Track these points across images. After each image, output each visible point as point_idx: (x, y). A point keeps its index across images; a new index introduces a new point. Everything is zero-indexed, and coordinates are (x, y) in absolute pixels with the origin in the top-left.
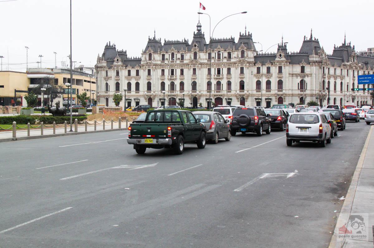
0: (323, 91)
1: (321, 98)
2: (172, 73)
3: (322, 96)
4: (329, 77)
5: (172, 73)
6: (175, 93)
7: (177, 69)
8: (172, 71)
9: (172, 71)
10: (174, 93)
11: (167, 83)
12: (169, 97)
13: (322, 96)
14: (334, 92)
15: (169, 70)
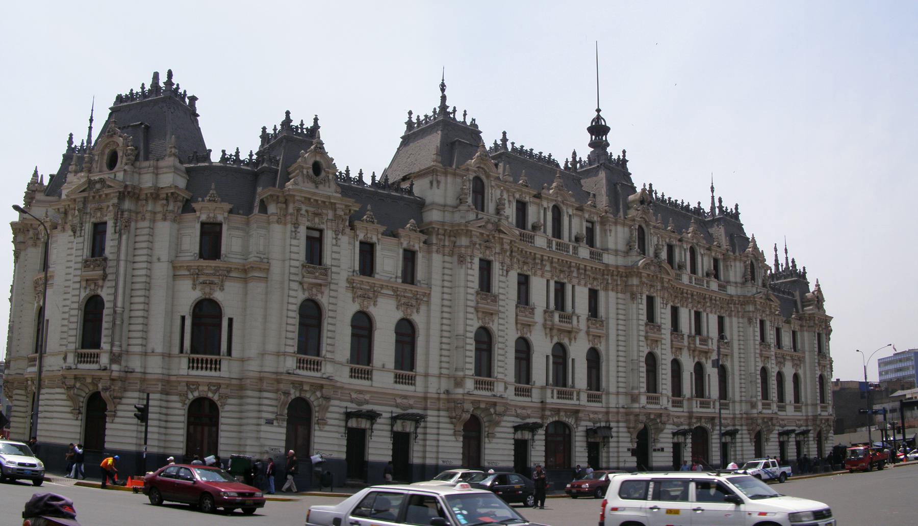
0: (822, 407)
1: (758, 428)
2: (560, 303)
3: (760, 421)
4: (781, 361)
5: (560, 303)
6: (578, 399)
7: (579, 284)
8: (560, 289)
9: (560, 289)
10: (575, 402)
11: (542, 348)
12: (551, 420)
13: (760, 421)
14: (795, 407)
15: (548, 281)
